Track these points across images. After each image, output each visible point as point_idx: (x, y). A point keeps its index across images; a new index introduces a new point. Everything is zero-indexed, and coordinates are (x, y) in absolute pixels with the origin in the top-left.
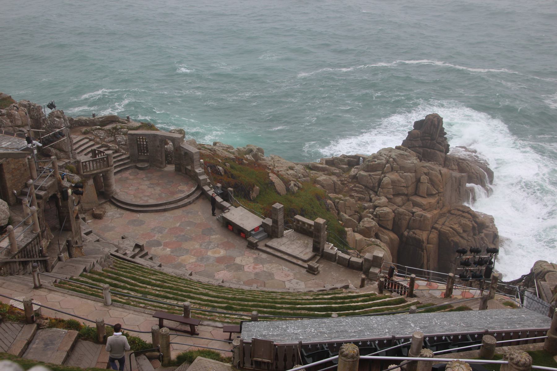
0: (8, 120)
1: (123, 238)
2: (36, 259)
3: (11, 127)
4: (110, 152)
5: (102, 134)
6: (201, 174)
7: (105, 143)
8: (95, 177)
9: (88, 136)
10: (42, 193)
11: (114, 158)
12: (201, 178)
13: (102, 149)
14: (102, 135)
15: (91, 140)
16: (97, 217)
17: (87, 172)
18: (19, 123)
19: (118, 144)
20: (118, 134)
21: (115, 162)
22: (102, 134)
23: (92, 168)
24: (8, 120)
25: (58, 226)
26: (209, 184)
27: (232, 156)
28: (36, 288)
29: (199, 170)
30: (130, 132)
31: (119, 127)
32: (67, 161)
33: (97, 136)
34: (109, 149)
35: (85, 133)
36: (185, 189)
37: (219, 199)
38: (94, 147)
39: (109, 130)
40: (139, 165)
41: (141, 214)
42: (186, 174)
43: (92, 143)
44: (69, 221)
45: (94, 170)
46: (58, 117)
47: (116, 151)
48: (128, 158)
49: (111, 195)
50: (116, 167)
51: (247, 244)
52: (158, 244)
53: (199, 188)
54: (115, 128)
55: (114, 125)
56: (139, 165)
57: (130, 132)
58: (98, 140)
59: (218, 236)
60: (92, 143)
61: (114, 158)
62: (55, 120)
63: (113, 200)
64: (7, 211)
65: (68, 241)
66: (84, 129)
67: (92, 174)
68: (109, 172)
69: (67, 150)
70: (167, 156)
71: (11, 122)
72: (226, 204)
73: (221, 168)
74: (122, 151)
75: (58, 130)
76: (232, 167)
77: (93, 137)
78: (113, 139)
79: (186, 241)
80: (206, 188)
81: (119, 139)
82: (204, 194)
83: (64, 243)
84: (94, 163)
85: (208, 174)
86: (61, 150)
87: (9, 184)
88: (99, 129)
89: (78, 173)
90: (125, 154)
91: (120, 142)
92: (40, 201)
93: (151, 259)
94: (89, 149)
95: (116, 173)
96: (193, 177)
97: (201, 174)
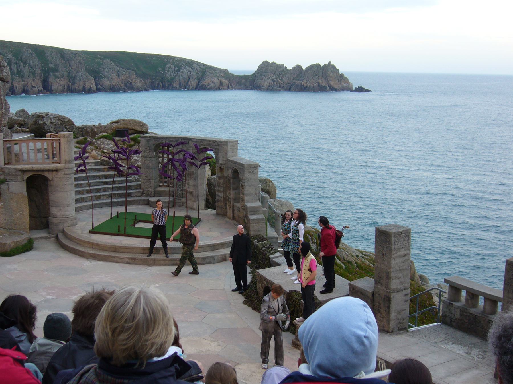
14: (107, 147)
49: (61, 227)
63: (61, 236)
67: (24, 171)
68: (60, 174)
81: (135, 158)
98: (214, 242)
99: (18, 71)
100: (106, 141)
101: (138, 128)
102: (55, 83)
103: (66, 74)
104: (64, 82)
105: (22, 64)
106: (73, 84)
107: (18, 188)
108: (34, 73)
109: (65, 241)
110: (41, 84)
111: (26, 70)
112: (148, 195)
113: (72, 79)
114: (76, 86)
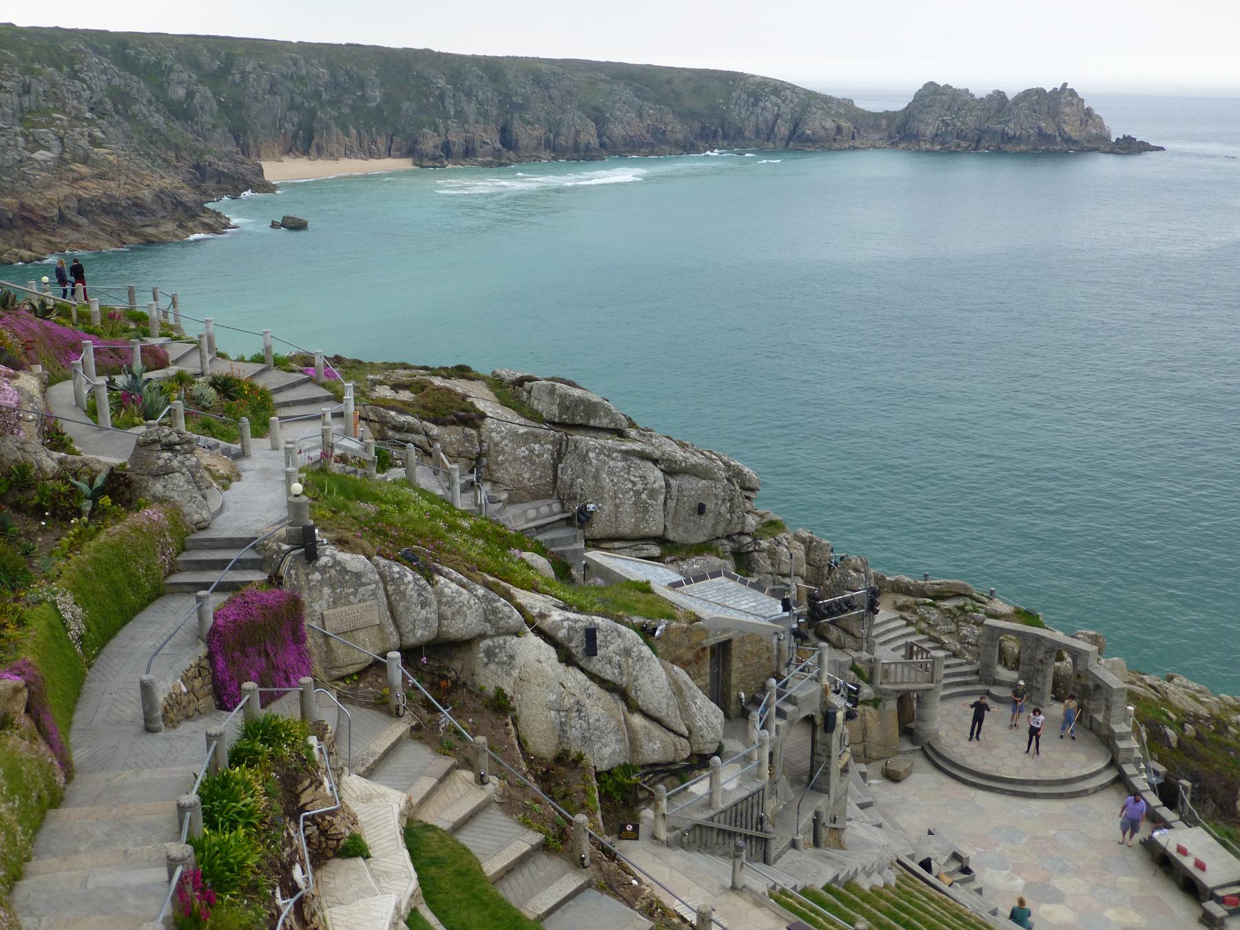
0: (769, 562)
1: (930, 833)
2: (749, 832)
4: (941, 654)
5: (934, 615)
6: (1123, 737)
7: (935, 634)
8: (903, 699)
9: (905, 614)
10: (789, 708)
11: (948, 666)
12: (1122, 745)
13: (926, 646)
14: (933, 618)
15: (909, 624)
16: (893, 777)
17: (889, 683)
18: (785, 569)
19: (962, 640)
20: (965, 621)
21: (946, 676)
22: (934, 615)
23: (899, 679)
24: (769, 562)
25: (805, 778)
26: (1136, 763)
27: (1203, 711)
28: (734, 888)
29: (1120, 728)
30: (989, 622)
31: (969, 607)
32: (855, 655)
33: (923, 619)
34: (942, 646)
35: (900, 608)
36: (1079, 761)
37: (1154, 800)
38: (912, 639)
39: (949, 611)
40: (995, 691)
41: (981, 793)
42: (1091, 729)
43: (911, 629)
44: (826, 773)
45: (902, 682)
46: (856, 570)
47: (955, 655)
48: (977, 673)
49: (926, 740)
50: (947, 686)
51: (1200, 913)
52: (1002, 864)
53: (1113, 763)
54: (961, 608)
55: (960, 602)
56: (995, 691)
57: (989, 622)
58: (924, 625)
59: (1137, 879)
61: (948, 666)
62: (849, 575)
64: (720, 728)
65: (817, 813)
66: (902, 599)
67: (897, 691)
68: (931, 693)
69: (859, 635)
70: (1056, 685)
71: (773, 565)
72: (1165, 812)
73: (1170, 732)
74: (968, 656)
75: (848, 595)
76: (1199, 737)
77: (914, 618)
78: (953, 627)
79: (1062, 871)
80: (1129, 769)
82: (1122, 781)
83: (811, 815)
84: (906, 670)
85: (1140, 739)
87: (735, 679)
88: (930, 604)
89: (870, 682)
90: (970, 663)
91: (966, 637)
92: (782, 723)
93: (979, 891)
94: (902, 642)
95: (944, 698)
96: (1107, 740)
97: (1123, 737)
98: (1085, 772)
99: (457, 112)
101: (962, 592)
102: (526, 134)
103: (543, 115)
104: (539, 132)
105: (464, 98)
106: (556, 137)
107: (892, 705)
108: (485, 115)
109: (940, 762)
110: (497, 137)
111: (471, 109)
112: (987, 683)
113: (554, 126)
114: (562, 140)
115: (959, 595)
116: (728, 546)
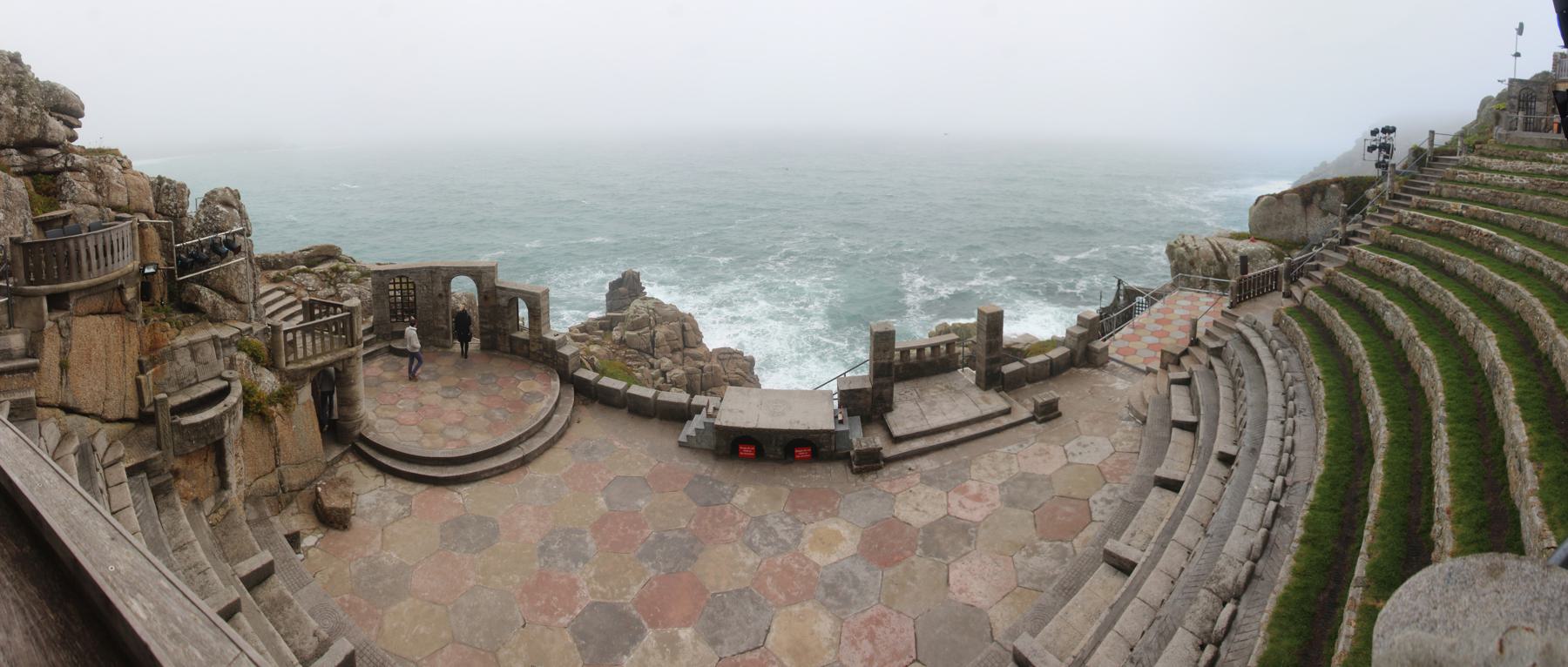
3: (96, 205)
5: (311, 281)
9: (282, 285)
17: (297, 361)
22: (311, 281)
23: (310, 353)
24: (90, 186)
32: (244, 326)
43: (291, 299)
55: (333, 264)
60: (291, 299)
62: (217, 212)
69: (243, 298)
71: (98, 192)
77: (292, 288)
78: (332, 291)
84: (309, 339)
86: (229, 296)
88: (304, 271)
100: (308, 276)
115: (328, 258)
116: (18, 159)
